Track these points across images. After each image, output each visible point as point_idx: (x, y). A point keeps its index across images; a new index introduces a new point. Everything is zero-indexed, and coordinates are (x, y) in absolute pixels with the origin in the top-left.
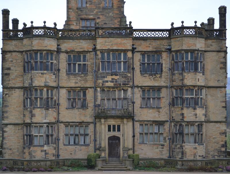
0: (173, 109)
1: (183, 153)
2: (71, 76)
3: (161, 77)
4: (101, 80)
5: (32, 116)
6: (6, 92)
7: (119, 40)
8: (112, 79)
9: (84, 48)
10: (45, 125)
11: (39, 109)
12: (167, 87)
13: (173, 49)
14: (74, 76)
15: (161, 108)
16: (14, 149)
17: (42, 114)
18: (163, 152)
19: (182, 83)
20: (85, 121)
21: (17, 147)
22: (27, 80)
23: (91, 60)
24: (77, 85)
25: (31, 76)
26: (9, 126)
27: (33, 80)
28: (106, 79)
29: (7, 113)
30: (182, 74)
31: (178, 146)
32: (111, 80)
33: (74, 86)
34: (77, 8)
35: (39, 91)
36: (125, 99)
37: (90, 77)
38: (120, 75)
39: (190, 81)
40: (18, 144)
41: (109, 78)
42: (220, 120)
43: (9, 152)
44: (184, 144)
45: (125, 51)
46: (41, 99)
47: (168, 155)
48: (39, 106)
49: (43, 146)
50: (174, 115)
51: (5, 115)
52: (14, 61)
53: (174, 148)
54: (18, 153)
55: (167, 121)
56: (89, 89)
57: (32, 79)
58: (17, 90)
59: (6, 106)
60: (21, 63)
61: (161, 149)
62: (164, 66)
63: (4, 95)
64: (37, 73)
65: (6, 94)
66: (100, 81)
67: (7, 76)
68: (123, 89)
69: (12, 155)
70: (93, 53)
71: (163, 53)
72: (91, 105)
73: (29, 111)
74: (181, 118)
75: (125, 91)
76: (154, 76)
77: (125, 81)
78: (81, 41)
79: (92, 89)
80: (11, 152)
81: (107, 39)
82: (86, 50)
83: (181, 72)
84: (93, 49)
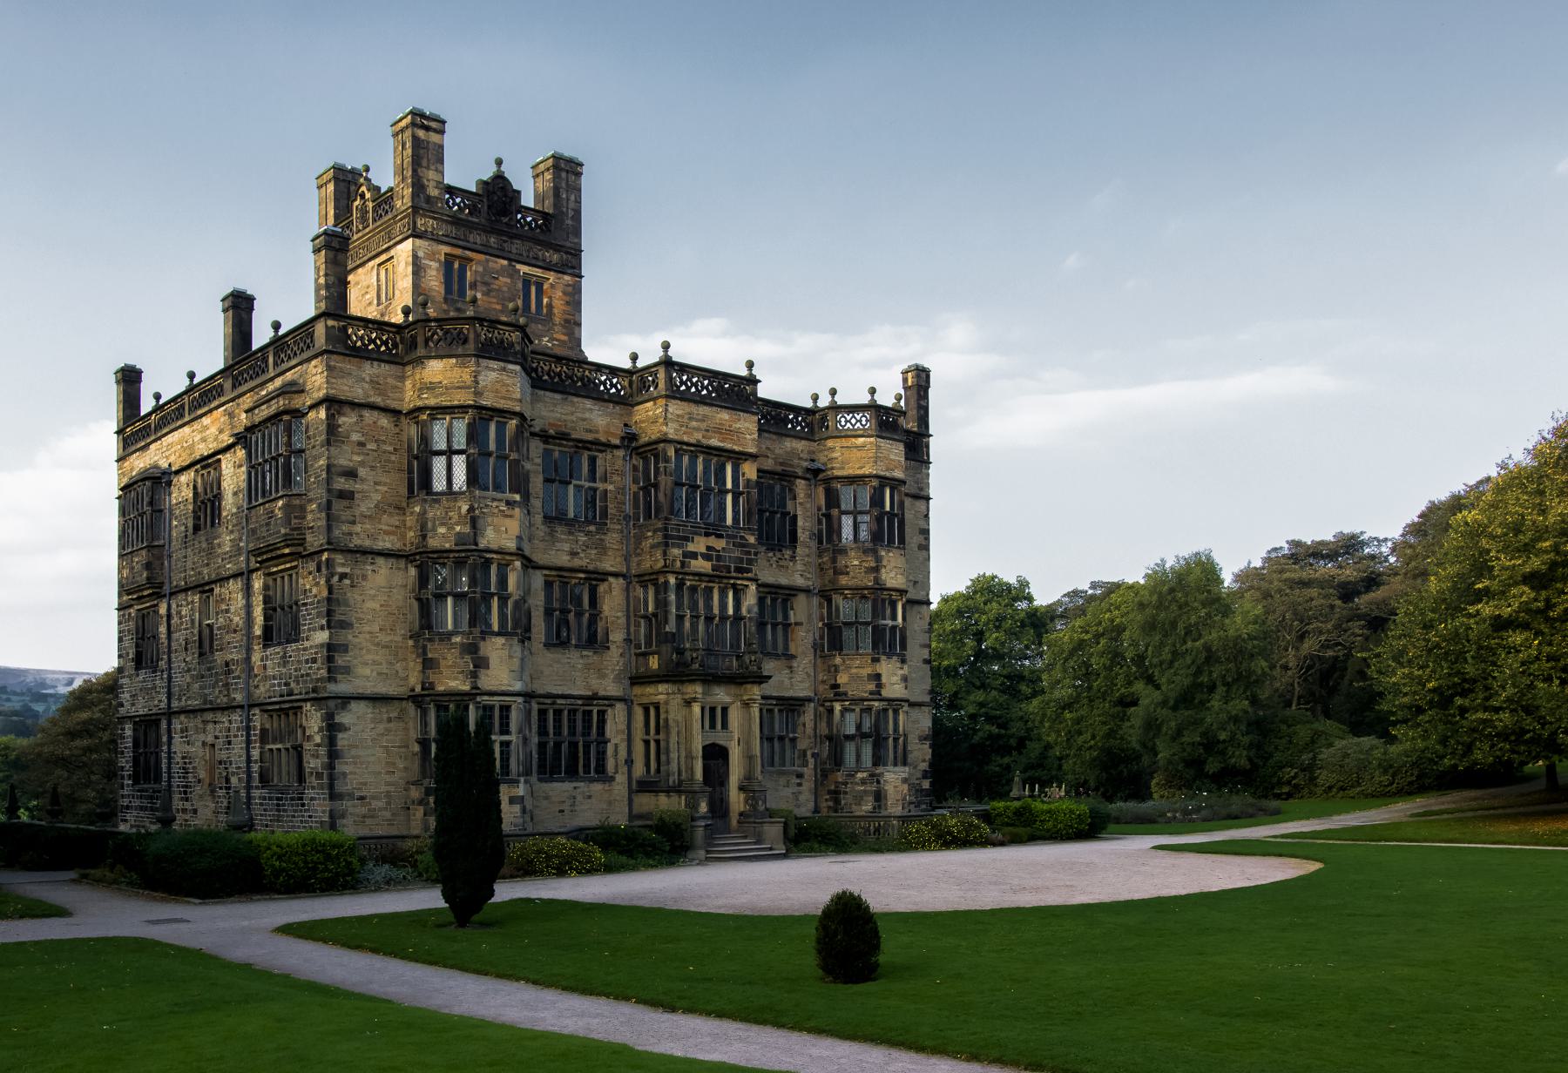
0: (838, 660)
1: (879, 796)
2: (559, 529)
3: (793, 558)
4: (679, 546)
5: (481, 663)
6: (343, 565)
7: (725, 415)
8: (709, 548)
9: (597, 432)
10: (520, 700)
11: (500, 641)
12: (807, 591)
13: (837, 473)
14: (565, 529)
15: (793, 657)
16: (373, 798)
17: (511, 657)
18: (802, 798)
19: (877, 580)
20: (602, 693)
21: (383, 788)
22: (442, 524)
23: (615, 478)
24: (577, 563)
25: (471, 509)
26: (354, 705)
27: (480, 522)
28: (691, 547)
29: (346, 651)
30: (875, 552)
31: (860, 775)
32: (703, 550)
33: (569, 565)
34: (446, 300)
35: (494, 569)
36: (738, 618)
37: (612, 538)
38: (728, 536)
39: (892, 574)
40: (388, 778)
41: (699, 545)
42: (920, 699)
43: (357, 811)
44: (880, 770)
45: (739, 457)
46: (503, 600)
47: (811, 805)
48: (496, 628)
49: (518, 782)
50: (842, 679)
51: (340, 660)
52: (369, 447)
53: (846, 784)
54: (388, 814)
55: (809, 700)
56: (611, 579)
57: (474, 522)
58: (381, 561)
59: (345, 625)
60: (393, 458)
61: (797, 789)
62: (800, 523)
63: (336, 578)
64: (494, 500)
65: (343, 576)
66: (676, 552)
67: (345, 503)
68: (734, 586)
69: (368, 821)
70: (620, 453)
71: (798, 481)
72: (617, 636)
73: (462, 644)
74: (872, 687)
75: (738, 592)
76: (778, 555)
77: (741, 560)
78: (588, 403)
79: (621, 580)
80: (364, 810)
81: (693, 408)
82: (603, 439)
83: (869, 545)
84: (623, 438)
